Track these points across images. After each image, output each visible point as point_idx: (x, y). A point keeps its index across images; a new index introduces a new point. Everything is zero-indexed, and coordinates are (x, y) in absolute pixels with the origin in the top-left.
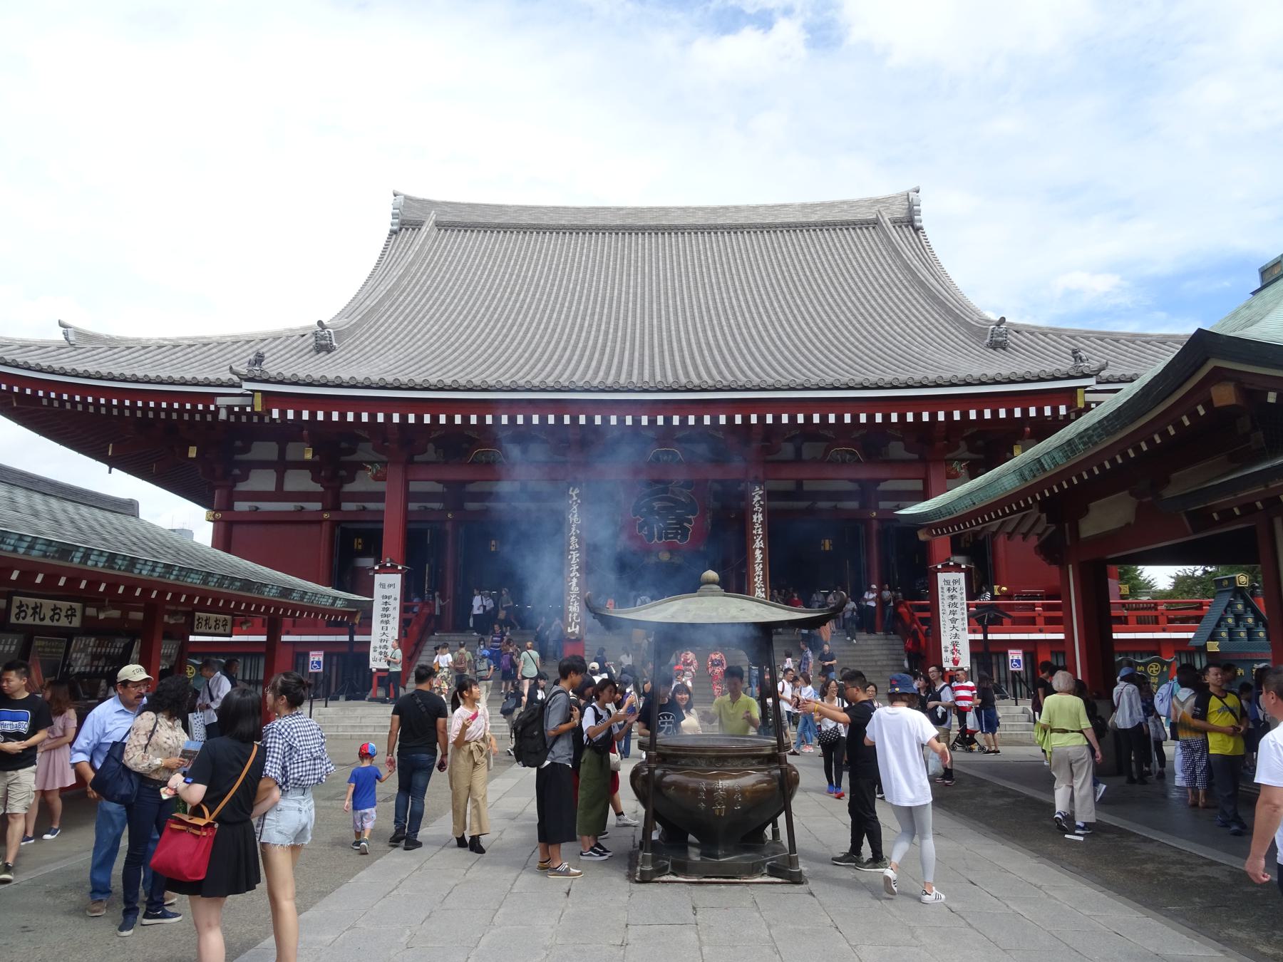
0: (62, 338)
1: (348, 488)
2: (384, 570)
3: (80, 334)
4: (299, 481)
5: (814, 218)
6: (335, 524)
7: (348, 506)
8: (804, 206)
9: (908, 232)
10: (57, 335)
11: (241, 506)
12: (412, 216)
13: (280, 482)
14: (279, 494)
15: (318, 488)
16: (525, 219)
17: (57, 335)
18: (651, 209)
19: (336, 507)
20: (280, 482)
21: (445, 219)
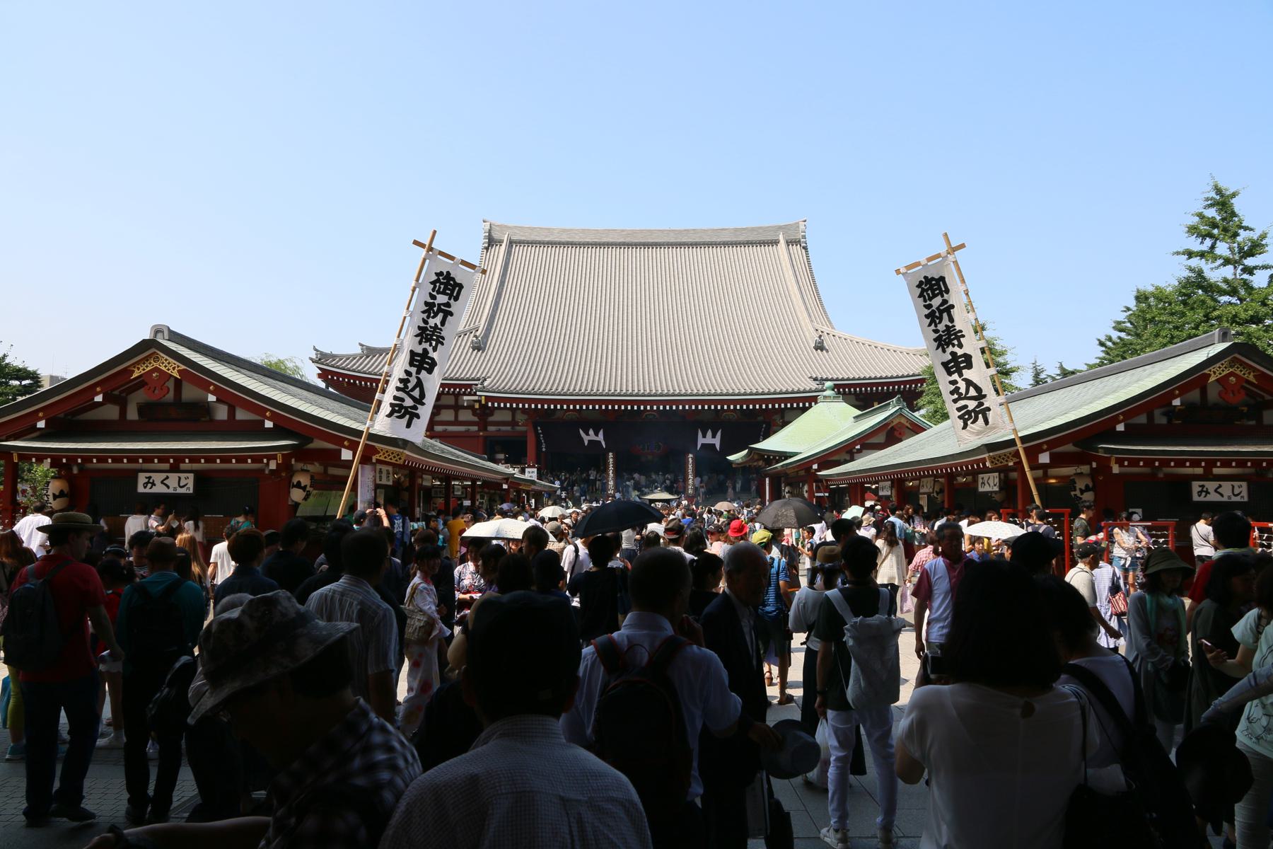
0: (359, 351)
1: (491, 419)
2: (529, 467)
3: (368, 348)
4: (465, 416)
5: (741, 238)
6: (485, 438)
7: (491, 428)
8: (736, 230)
9: (796, 250)
10: (358, 350)
11: (438, 428)
12: (496, 235)
13: (456, 416)
14: (456, 422)
15: (476, 419)
16: (564, 238)
17: (358, 350)
18: (641, 231)
19: (485, 429)
20: (456, 416)
21: (514, 238)
